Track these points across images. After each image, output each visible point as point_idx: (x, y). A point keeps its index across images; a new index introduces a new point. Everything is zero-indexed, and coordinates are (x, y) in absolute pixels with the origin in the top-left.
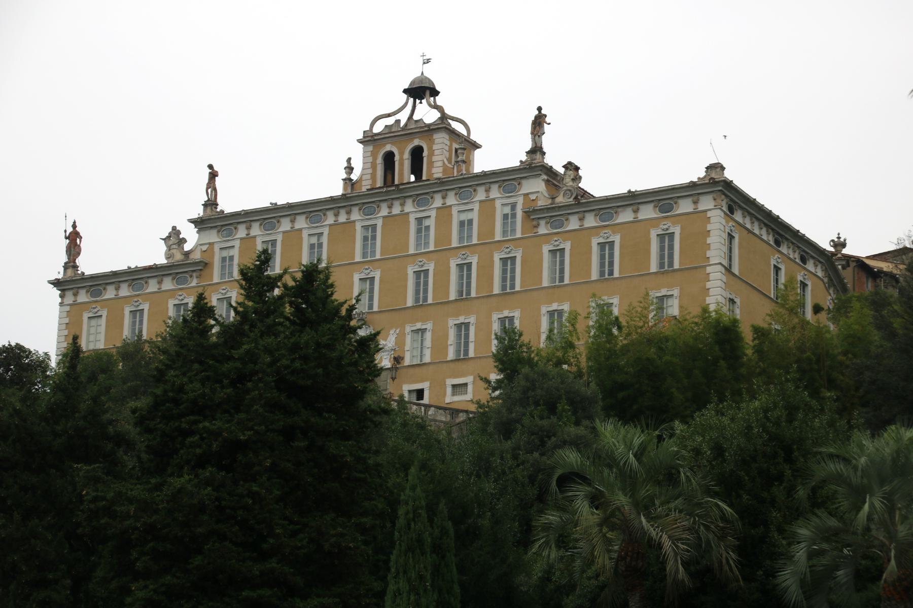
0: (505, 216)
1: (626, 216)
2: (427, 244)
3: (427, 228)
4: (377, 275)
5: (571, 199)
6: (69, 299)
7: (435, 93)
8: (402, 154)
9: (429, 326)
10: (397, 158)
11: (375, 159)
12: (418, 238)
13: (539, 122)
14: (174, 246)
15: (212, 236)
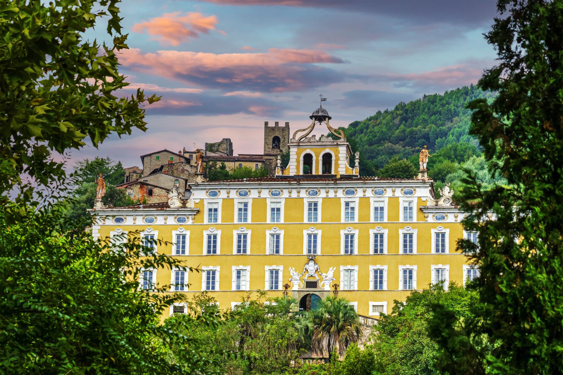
0: (405, 208)
3: (353, 208)
5: (449, 205)
8: (317, 156)
9: (356, 268)
10: (314, 158)
11: (299, 157)
12: (347, 213)
14: (175, 198)
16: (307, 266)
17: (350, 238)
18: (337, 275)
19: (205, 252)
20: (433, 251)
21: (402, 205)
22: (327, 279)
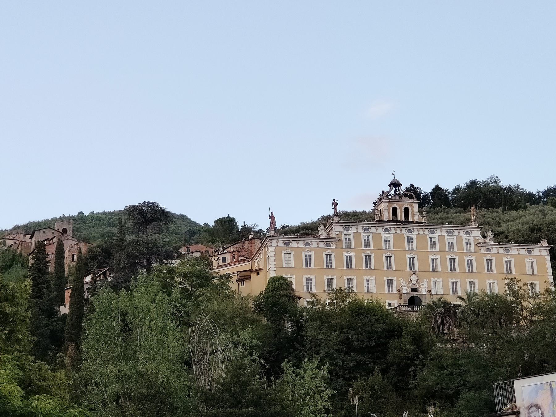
0: (467, 243)
3: (435, 242)
9: (441, 280)
11: (389, 209)
12: (431, 245)
16: (411, 278)
18: (429, 284)
19: (345, 267)
20: (486, 271)
21: (465, 241)
22: (423, 286)
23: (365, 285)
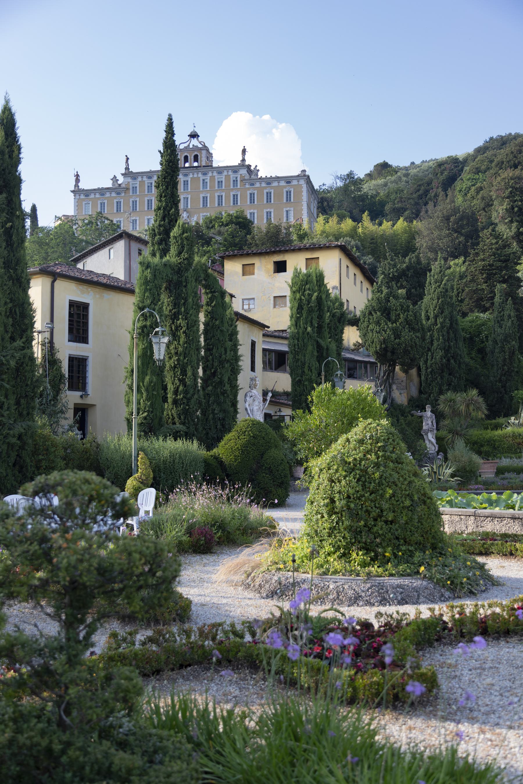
0: (234, 181)
1: (275, 184)
2: (206, 188)
4: (189, 197)
6: (78, 197)
7: (198, 136)
12: (203, 186)
13: (244, 151)
15: (129, 180)
17: (205, 199)
20: (248, 203)
23: (285, 215)
